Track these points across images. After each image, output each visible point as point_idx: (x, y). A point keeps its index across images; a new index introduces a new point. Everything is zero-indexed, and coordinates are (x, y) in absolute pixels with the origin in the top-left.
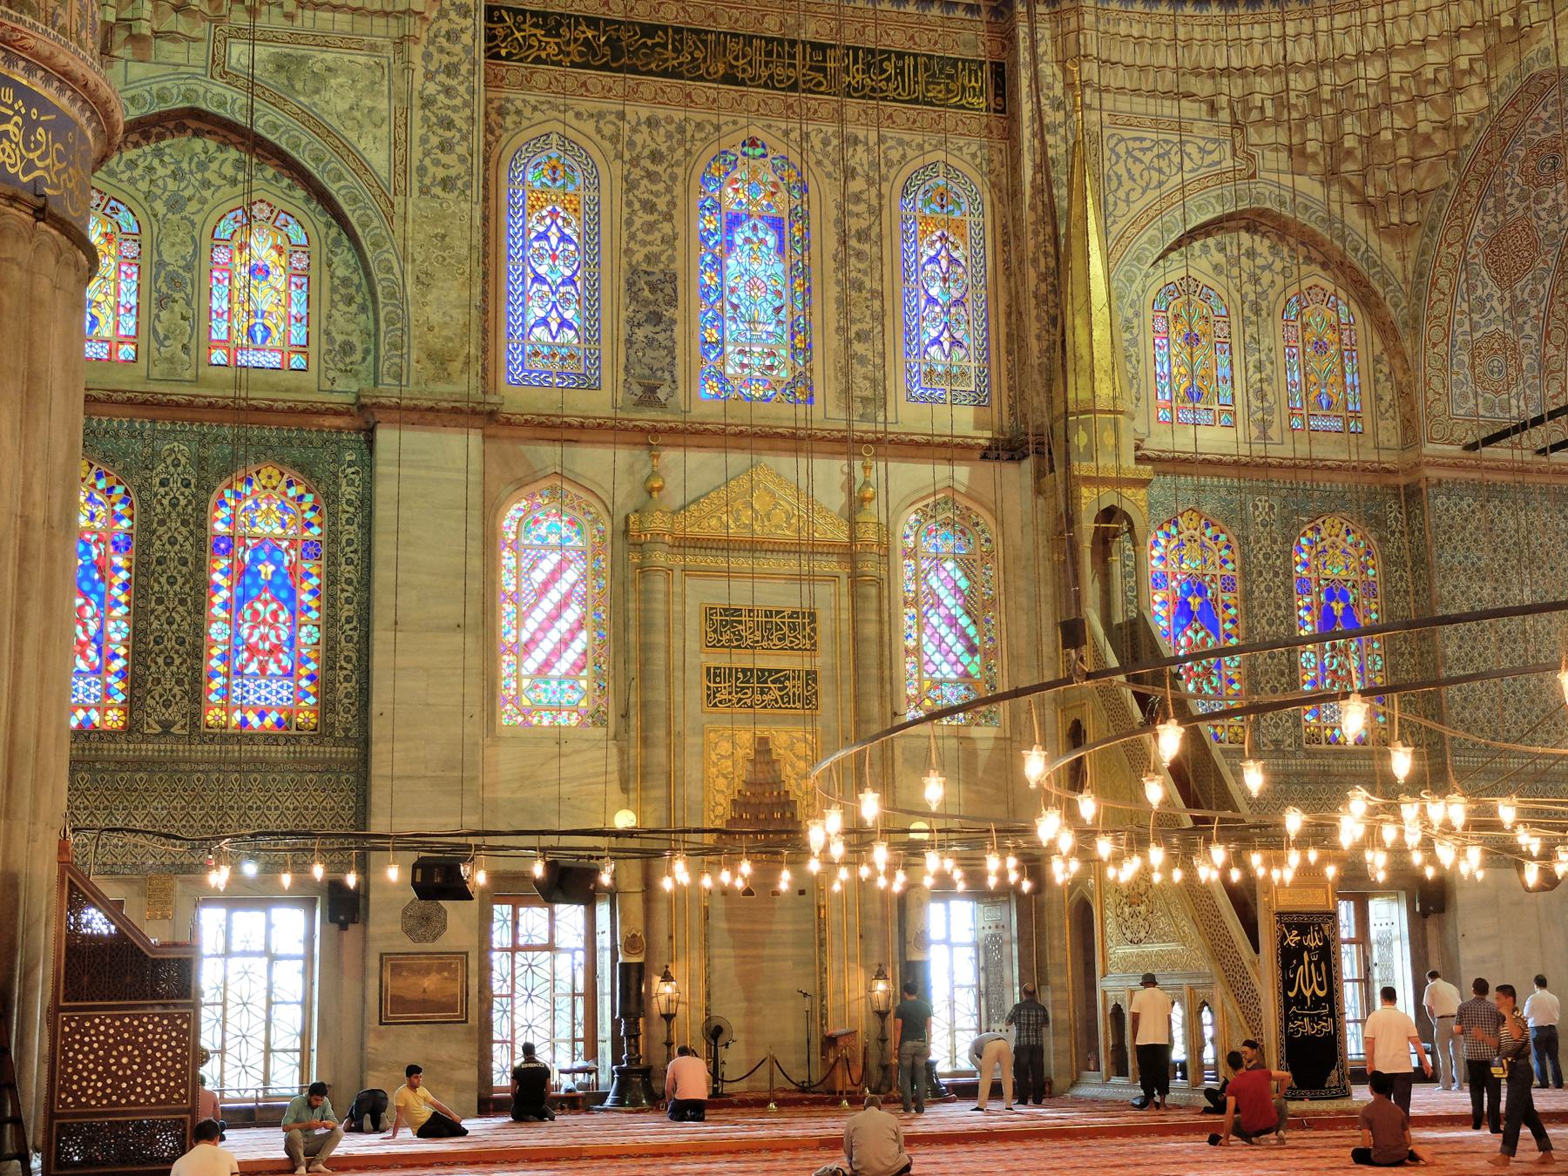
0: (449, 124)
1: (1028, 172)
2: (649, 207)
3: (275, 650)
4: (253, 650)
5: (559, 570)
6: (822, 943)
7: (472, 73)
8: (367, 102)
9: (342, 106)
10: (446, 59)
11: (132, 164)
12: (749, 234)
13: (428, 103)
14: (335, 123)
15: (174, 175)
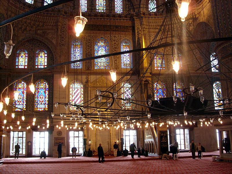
0: (63, 38)
1: (137, 39)
2: (88, 46)
3: (43, 101)
4: (40, 101)
5: (77, 91)
6: (111, 136)
7: (66, 31)
8: (53, 36)
9: (50, 37)
10: (63, 30)
11: (27, 45)
12: (101, 49)
13: (61, 35)
14: (50, 39)
15: (32, 46)
